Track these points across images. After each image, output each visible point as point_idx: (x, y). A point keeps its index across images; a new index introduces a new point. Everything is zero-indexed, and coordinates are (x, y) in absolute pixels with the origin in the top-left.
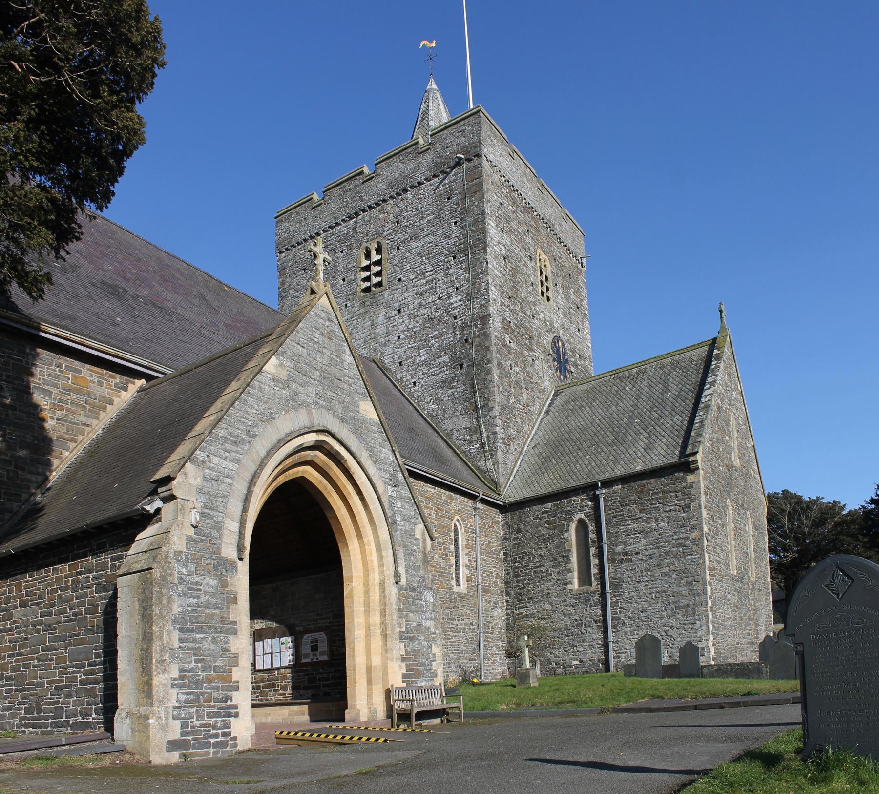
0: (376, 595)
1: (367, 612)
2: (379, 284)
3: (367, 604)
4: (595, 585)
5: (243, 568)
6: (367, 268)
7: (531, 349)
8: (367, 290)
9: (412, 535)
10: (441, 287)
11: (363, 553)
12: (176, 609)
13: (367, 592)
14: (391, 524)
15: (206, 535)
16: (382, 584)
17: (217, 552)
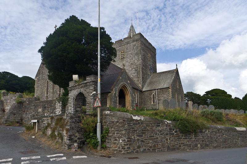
0: (129, 101)
1: (128, 103)
2: (124, 57)
3: (128, 102)
4: (155, 103)
5: (118, 98)
6: (122, 55)
7: (147, 68)
8: (122, 58)
9: (133, 95)
10: (134, 59)
11: (128, 97)
12: (113, 101)
13: (128, 101)
14: (131, 94)
15: (115, 94)
16: (130, 100)
17: (116, 95)
